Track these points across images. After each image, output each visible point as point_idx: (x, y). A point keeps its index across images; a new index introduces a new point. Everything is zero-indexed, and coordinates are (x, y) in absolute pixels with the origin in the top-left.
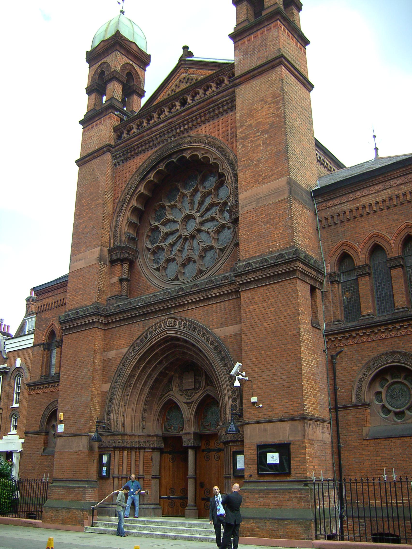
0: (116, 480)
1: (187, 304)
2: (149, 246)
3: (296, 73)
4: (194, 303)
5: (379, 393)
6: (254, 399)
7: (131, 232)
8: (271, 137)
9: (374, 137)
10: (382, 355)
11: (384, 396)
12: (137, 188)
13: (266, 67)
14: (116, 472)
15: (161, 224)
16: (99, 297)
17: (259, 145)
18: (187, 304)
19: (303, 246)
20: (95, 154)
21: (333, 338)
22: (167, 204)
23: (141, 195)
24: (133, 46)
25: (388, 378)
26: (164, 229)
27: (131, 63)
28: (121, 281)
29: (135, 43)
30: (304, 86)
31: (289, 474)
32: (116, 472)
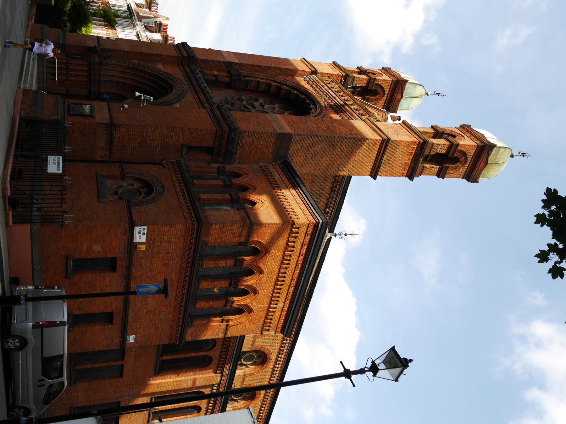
0: (65, 61)
1: (198, 95)
2: (243, 97)
3: (380, 157)
4: (199, 98)
5: (133, 185)
6: (126, 106)
7: (253, 84)
8: (324, 130)
9: (346, 235)
10: (162, 184)
11: (130, 187)
12: (286, 85)
13: (380, 132)
14: (71, 61)
15: (260, 103)
16: (202, 60)
17: (317, 125)
18: (198, 95)
19: (242, 144)
20: (309, 65)
21: (176, 164)
22: (276, 106)
23: (280, 88)
24: (399, 96)
25: (145, 190)
26: (256, 104)
27: (386, 95)
28: (215, 76)
29: (402, 97)
30: (373, 168)
31: (69, 114)
32: (71, 61)
